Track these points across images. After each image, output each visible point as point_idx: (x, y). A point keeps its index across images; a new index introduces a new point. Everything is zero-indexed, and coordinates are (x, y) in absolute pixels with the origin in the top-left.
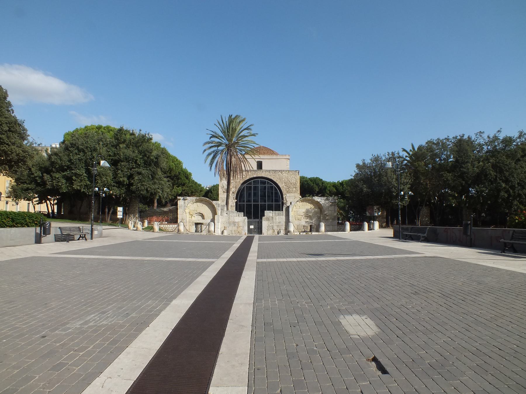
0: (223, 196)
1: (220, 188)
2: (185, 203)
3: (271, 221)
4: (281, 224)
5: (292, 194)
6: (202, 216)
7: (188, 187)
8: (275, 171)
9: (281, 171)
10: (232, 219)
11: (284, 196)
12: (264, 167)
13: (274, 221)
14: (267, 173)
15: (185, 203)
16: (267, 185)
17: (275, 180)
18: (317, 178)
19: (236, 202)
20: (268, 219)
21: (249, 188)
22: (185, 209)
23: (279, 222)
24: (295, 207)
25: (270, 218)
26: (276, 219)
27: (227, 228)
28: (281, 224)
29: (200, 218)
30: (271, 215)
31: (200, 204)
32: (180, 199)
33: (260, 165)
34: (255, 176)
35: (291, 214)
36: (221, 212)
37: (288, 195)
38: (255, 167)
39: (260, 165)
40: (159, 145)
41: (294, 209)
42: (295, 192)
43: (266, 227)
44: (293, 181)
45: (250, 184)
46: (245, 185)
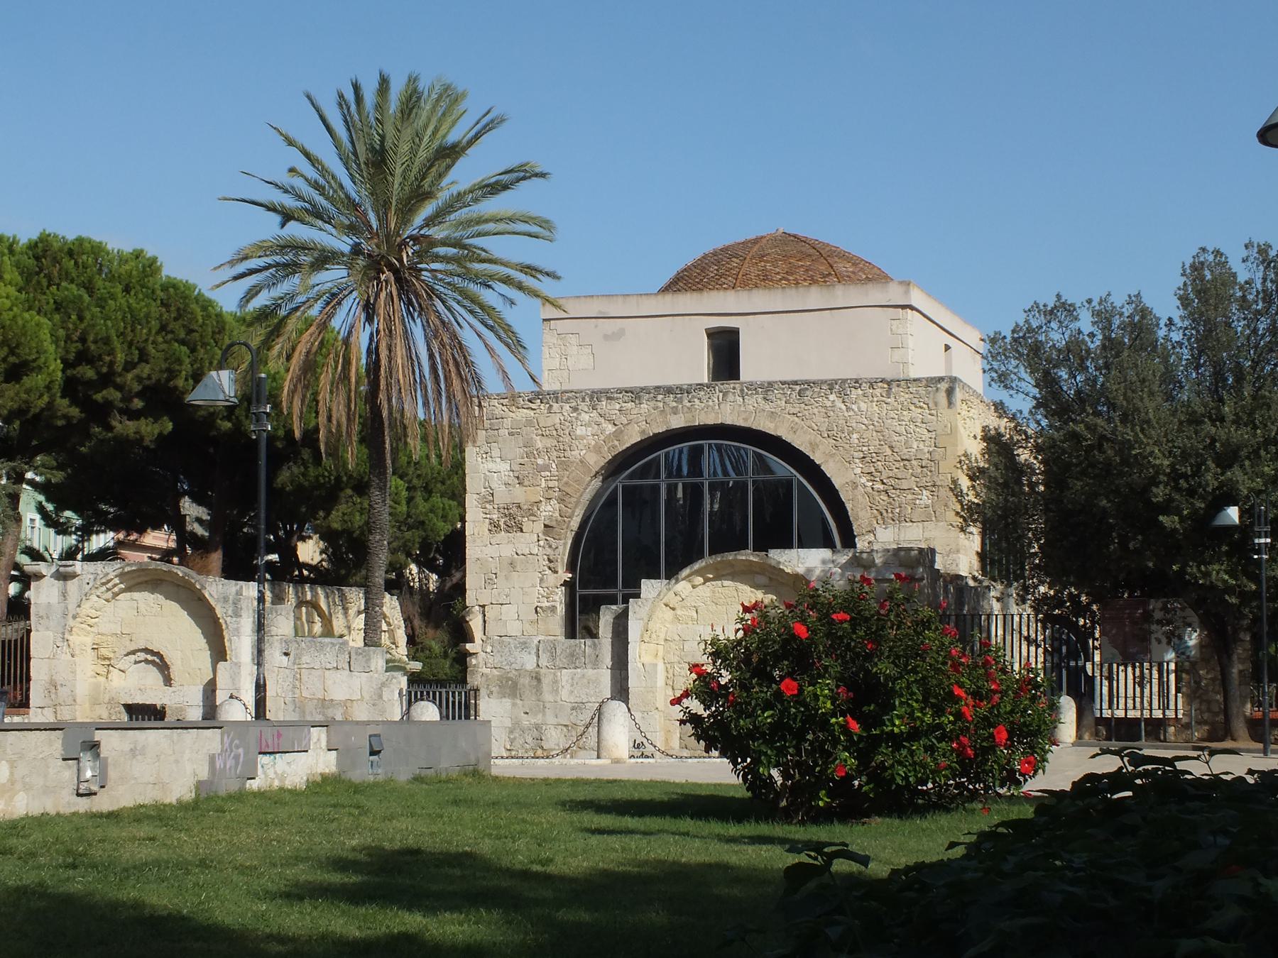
0: (491, 551)
1: (471, 501)
2: (64, 595)
6: (162, 666)
8: (802, 387)
13: (547, 697)
14: (754, 401)
15: (64, 595)
17: (800, 441)
20: (509, 687)
21: (639, 501)
22: (65, 632)
25: (525, 681)
29: (154, 675)
31: (147, 600)
32: (39, 577)
33: (725, 353)
34: (677, 422)
35: (637, 653)
38: (698, 366)
39: (725, 353)
40: (151, 267)
44: (920, 445)
45: (651, 470)
46: (620, 482)
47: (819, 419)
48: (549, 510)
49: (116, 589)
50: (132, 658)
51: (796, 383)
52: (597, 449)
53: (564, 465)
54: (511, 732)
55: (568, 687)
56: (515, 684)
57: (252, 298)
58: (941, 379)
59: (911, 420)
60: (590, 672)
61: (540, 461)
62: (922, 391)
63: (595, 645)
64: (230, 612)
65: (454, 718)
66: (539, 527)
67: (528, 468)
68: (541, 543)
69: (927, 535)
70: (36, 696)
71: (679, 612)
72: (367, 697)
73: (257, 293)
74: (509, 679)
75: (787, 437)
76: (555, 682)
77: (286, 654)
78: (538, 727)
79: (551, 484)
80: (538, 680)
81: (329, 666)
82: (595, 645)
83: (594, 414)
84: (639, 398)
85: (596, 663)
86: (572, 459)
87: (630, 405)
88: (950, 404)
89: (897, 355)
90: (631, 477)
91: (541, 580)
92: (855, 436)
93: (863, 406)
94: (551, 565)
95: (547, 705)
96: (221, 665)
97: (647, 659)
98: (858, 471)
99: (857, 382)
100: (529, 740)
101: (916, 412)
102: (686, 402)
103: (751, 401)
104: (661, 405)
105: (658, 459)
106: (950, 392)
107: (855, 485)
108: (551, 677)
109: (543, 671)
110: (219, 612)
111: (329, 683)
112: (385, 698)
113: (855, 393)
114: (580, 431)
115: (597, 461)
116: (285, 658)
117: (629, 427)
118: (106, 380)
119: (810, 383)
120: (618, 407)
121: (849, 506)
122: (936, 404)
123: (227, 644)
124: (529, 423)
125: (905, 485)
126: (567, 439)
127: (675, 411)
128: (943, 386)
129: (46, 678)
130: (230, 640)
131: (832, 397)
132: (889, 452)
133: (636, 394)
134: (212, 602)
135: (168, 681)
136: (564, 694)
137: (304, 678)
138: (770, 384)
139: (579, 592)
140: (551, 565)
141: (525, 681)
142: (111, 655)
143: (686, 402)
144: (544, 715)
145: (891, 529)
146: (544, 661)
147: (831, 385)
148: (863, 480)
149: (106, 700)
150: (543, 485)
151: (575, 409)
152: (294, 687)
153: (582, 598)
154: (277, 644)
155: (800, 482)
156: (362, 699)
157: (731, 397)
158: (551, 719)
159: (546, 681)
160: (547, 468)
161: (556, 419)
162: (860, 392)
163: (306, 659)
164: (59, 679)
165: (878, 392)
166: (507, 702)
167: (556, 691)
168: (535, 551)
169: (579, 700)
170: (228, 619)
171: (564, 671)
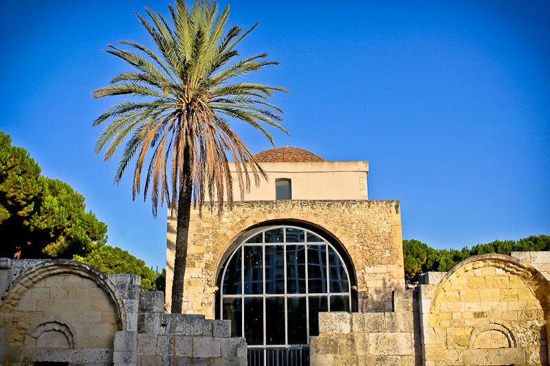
5: (383, 269)
7: (111, 268)
8: (330, 203)
11: (358, 274)
12: (296, 194)
13: (360, 352)
16: (305, 244)
17: (329, 227)
19: (217, 294)
20: (333, 347)
21: (253, 255)
24: (441, 294)
25: (343, 341)
30: (346, 329)
33: (284, 189)
34: (271, 217)
36: (141, 319)
37: (369, 270)
39: (284, 189)
41: (442, 305)
42: (390, 261)
47: (337, 217)
48: (208, 257)
49: (35, 279)
50: (43, 328)
51: (326, 201)
53: (216, 235)
55: (374, 345)
59: (380, 219)
60: (389, 335)
61: (204, 234)
62: (384, 206)
63: (392, 316)
64: (126, 295)
65: (275, 365)
66: (203, 265)
67: (198, 237)
68: (204, 272)
69: (389, 270)
71: (447, 293)
72: (225, 355)
74: (332, 340)
75: (324, 225)
76: (365, 341)
77: (163, 325)
79: (209, 245)
80: (352, 340)
82: (392, 316)
83: (231, 212)
84: (252, 206)
85: (393, 328)
86: (220, 233)
87: (248, 209)
88: (397, 212)
90: (248, 242)
91: (204, 290)
92: (354, 225)
94: (209, 283)
95: (360, 358)
97: (432, 324)
98: (356, 241)
101: (382, 215)
102: (275, 208)
103: (305, 209)
104: (263, 209)
105: (261, 234)
108: (362, 338)
109: (355, 335)
110: (117, 294)
111: (197, 345)
112: (239, 355)
115: (232, 235)
117: (247, 219)
120: (242, 209)
123: (123, 318)
125: (378, 247)
126: (218, 223)
127: (270, 212)
128: (394, 204)
130: (125, 316)
131: (343, 208)
132: (370, 233)
134: (113, 289)
135: (72, 345)
136: (372, 350)
138: (314, 201)
139: (223, 296)
140: (209, 283)
141: (343, 341)
142: (28, 327)
143: (275, 208)
145: (372, 268)
146: (356, 327)
147: (343, 202)
148: (359, 245)
149: (22, 359)
152: (170, 349)
153: (224, 299)
154: (157, 318)
155: (329, 247)
156: (221, 357)
157: (296, 207)
159: (358, 341)
160: (207, 237)
162: (355, 206)
165: (364, 206)
167: (366, 348)
168: (201, 276)
169: (382, 353)
170: (124, 301)
171: (371, 334)
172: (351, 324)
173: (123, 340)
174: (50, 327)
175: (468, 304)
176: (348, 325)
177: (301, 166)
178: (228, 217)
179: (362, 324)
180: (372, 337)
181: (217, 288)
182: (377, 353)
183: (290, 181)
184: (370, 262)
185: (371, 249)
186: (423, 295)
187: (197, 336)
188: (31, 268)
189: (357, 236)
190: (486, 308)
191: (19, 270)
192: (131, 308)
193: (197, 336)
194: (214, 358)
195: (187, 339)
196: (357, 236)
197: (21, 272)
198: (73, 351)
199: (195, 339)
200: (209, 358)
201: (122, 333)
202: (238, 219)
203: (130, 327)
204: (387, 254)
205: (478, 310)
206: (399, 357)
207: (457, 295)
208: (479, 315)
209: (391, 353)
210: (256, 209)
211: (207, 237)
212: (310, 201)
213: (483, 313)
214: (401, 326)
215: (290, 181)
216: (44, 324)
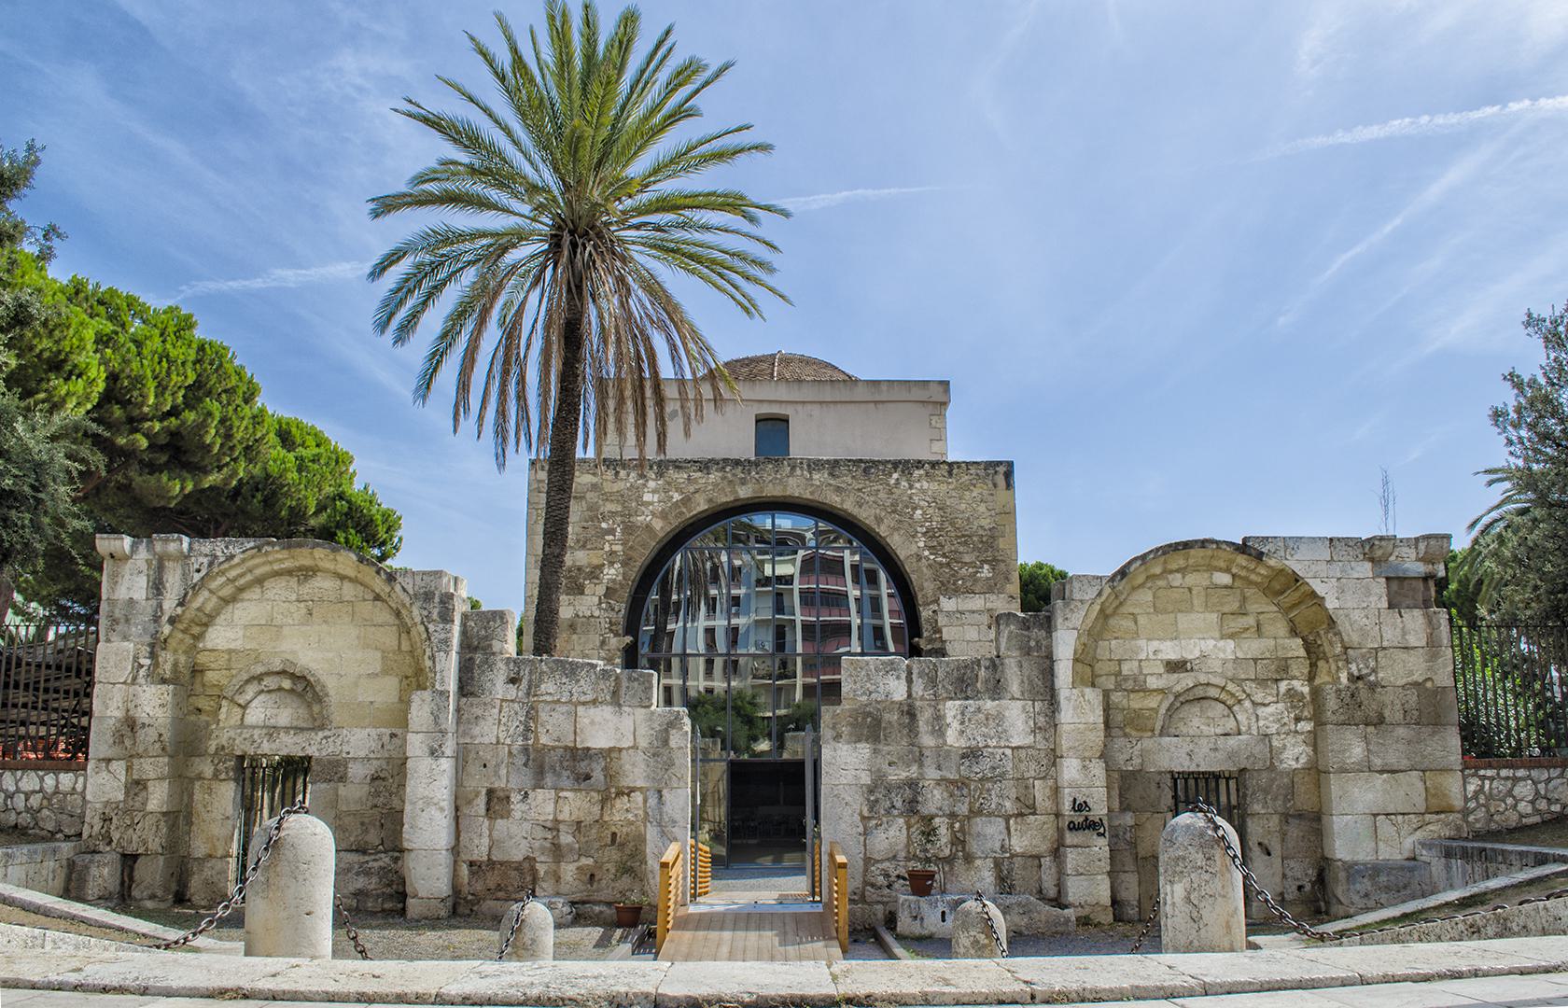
3: (896, 747)
4: (984, 766)
5: (977, 602)
8: (868, 467)
9: (906, 466)
10: (553, 730)
11: (925, 613)
13: (927, 740)
17: (865, 515)
18: (1040, 566)
20: (870, 727)
23: (972, 754)
26: (939, 728)
27: (517, 807)
28: (984, 766)
34: (745, 492)
36: (466, 669)
37: (948, 604)
43: (858, 803)
48: (611, 573)
52: (664, 515)
53: (629, 529)
54: (871, 792)
55: (956, 725)
56: (877, 722)
57: (390, 265)
58: (999, 463)
60: (989, 705)
61: (604, 525)
64: (435, 616)
66: (601, 590)
69: (989, 605)
70: (99, 743)
72: (643, 743)
73: (399, 259)
74: (869, 714)
76: (938, 717)
78: (912, 784)
80: (910, 712)
81: (583, 699)
89: (936, 447)
92: (919, 512)
93: (925, 485)
95: (927, 753)
96: (417, 697)
99: (919, 464)
100: (899, 804)
106: (1009, 475)
107: (919, 558)
109: (918, 703)
112: (673, 744)
113: (917, 473)
114: (647, 497)
116: (512, 692)
118: (133, 423)
119: (875, 463)
121: (914, 577)
122: (995, 485)
123: (428, 663)
124: (594, 487)
125: (967, 559)
127: (743, 482)
128: (1002, 469)
129: (119, 714)
130: (433, 658)
133: (705, 465)
136: (952, 738)
137: (543, 716)
138: (836, 462)
144: (921, 765)
147: (896, 464)
149: (212, 749)
150: (607, 548)
151: (642, 476)
152: (527, 729)
154: (501, 665)
156: (635, 747)
157: (798, 472)
158: (932, 773)
159: (924, 718)
160: (611, 531)
161: (620, 486)
163: (548, 687)
164: (141, 716)
166: (865, 749)
167: (939, 731)
168: (597, 613)
171: (949, 704)
172: (909, 681)
173: (427, 709)
174: (270, 682)
175: (1155, 644)
176: (903, 683)
177: (807, 393)
178: (654, 492)
179: (932, 681)
180: (951, 709)
181: (629, 639)
182: (963, 743)
183: (785, 421)
184: (950, 588)
185: (953, 558)
186: (1060, 621)
187: (584, 704)
188: (232, 557)
189: (924, 534)
190: (1191, 650)
191: (206, 561)
192: (446, 642)
193: (584, 704)
194: (620, 750)
195: (564, 709)
196: (924, 534)
197: (211, 564)
198: (321, 734)
199: (580, 708)
200: (611, 750)
201: (427, 695)
202: (677, 497)
203: (443, 682)
204: (986, 571)
205: (1173, 656)
206: (1008, 752)
207: (1131, 624)
208: (1176, 666)
209: (993, 743)
210: (714, 476)
211: (611, 531)
212: (828, 462)
213: (1185, 662)
214: (1015, 688)
215: (785, 421)
216: (259, 678)
